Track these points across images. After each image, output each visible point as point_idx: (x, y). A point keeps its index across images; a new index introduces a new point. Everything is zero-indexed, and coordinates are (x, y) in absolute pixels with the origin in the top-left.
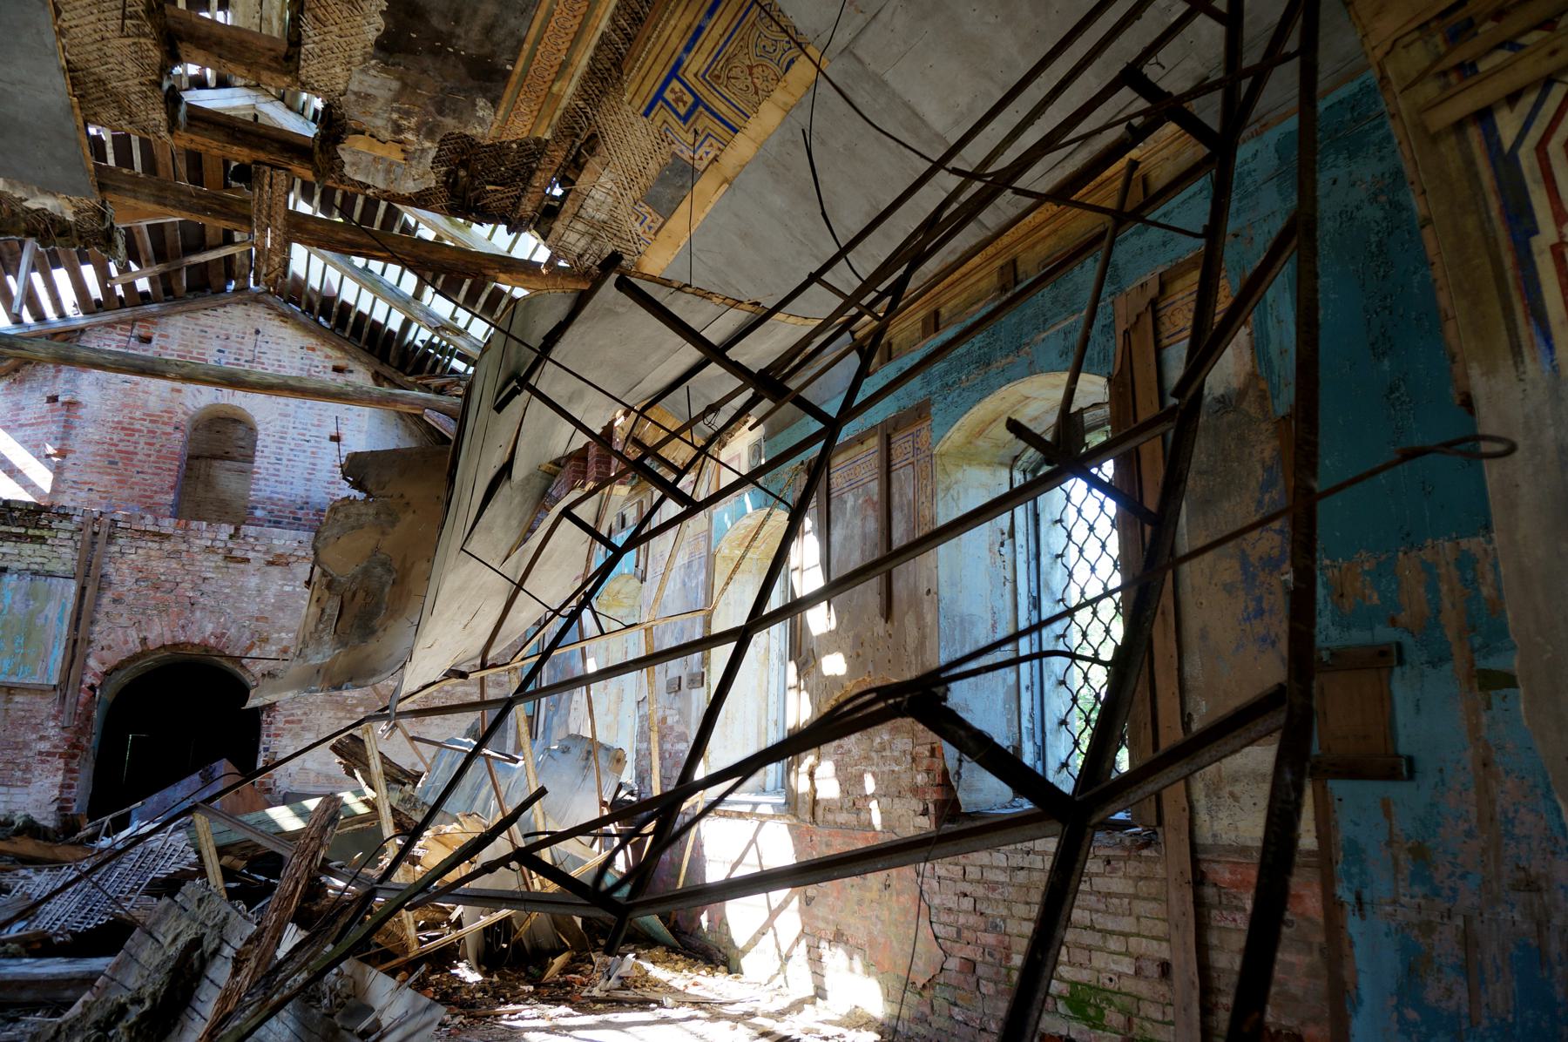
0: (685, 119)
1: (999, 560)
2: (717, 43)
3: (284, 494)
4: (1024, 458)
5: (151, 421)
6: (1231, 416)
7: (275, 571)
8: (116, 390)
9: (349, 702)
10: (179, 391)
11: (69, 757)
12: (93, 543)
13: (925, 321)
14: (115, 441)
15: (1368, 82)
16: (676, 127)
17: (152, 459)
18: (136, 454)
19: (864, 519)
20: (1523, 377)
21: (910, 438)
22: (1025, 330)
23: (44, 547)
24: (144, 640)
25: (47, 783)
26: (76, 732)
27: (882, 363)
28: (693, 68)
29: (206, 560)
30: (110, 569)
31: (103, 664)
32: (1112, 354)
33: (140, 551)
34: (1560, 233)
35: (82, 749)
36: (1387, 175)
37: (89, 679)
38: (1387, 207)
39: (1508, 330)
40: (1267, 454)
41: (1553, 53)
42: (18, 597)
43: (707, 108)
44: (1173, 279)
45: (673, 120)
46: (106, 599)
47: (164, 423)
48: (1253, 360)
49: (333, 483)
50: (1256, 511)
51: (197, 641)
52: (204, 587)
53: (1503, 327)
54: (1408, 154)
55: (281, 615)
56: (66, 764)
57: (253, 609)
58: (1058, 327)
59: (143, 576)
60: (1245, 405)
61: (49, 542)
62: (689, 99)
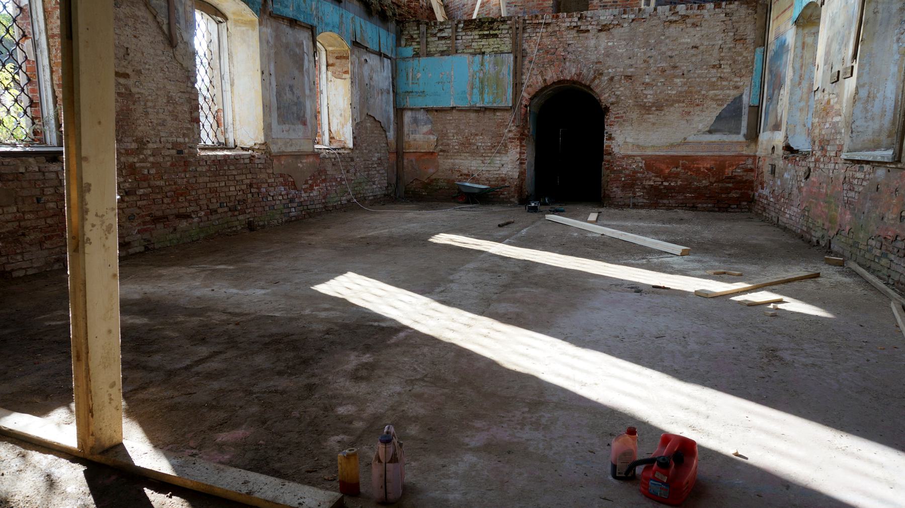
7: (603, 34)
9: (647, 105)
11: (521, 139)
12: (517, 34)
23: (498, 39)
24: (545, 80)
25: (514, 152)
26: (522, 128)
29: (568, 34)
30: (525, 46)
31: (529, 94)
33: (538, 34)
35: (527, 136)
37: (524, 103)
42: (491, 66)
46: (526, 62)
51: (568, 78)
52: (570, 49)
55: (608, 59)
56: (521, 143)
57: (593, 58)
59: (541, 47)
61: (499, 36)
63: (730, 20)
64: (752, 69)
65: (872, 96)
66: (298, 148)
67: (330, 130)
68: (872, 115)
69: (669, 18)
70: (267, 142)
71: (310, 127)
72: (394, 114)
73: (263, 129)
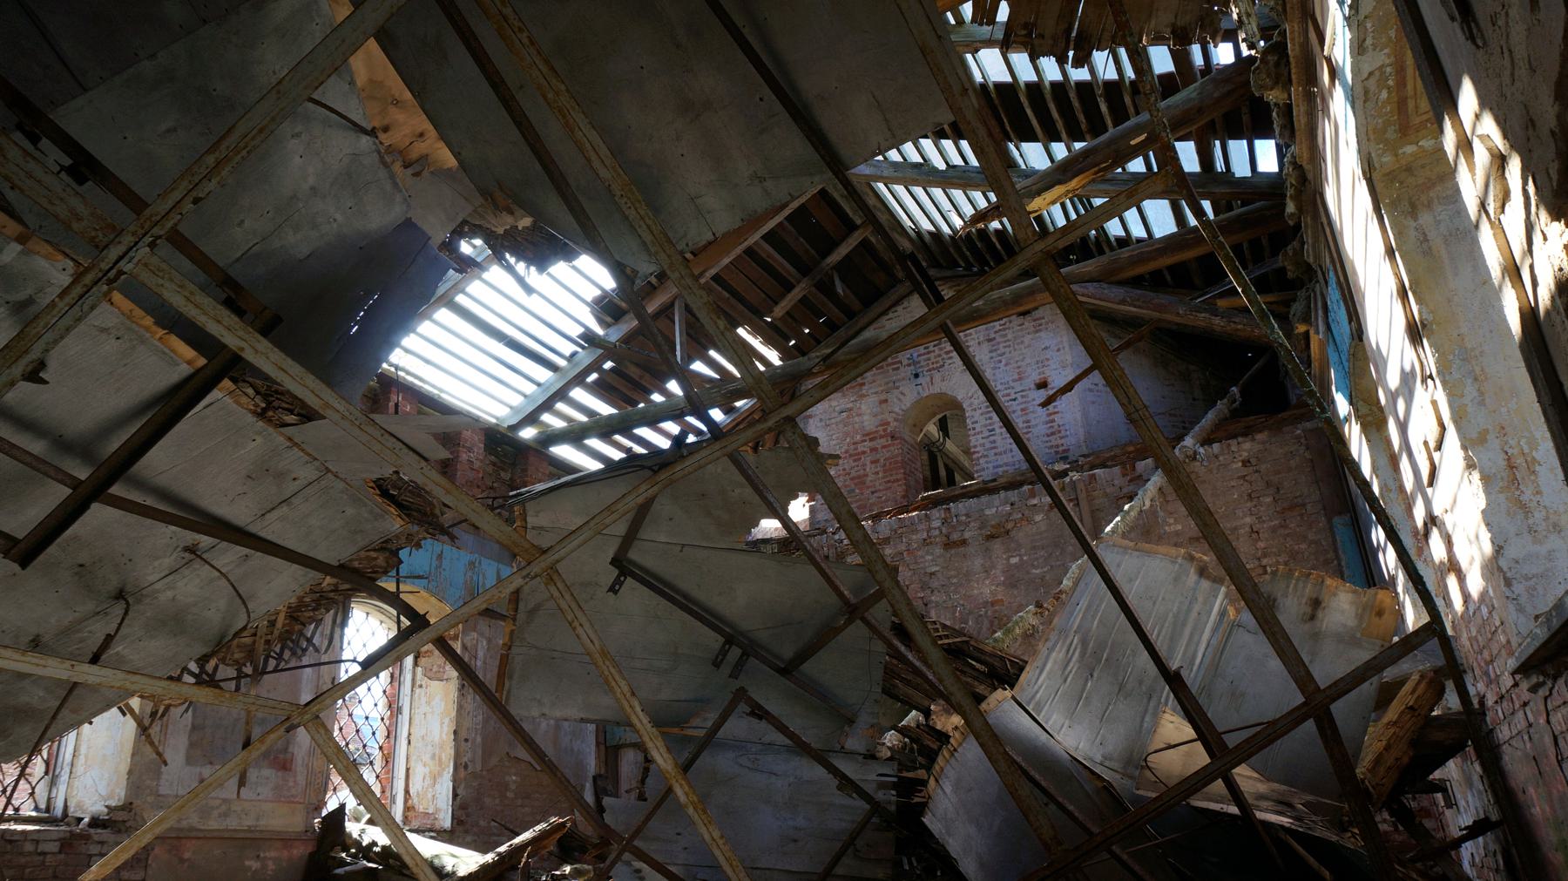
3: (1006, 464)
5: (871, 440)
7: (997, 546)
8: (837, 424)
10: (886, 401)
14: (848, 471)
17: (881, 475)
18: (867, 475)
29: (928, 553)
47: (881, 437)
49: (1053, 434)
52: (935, 584)
63: (1257, 471)
64: (1339, 565)
65: (1520, 461)
66: (248, 822)
67: (407, 792)
68: (1547, 519)
69: (1125, 490)
70: (137, 802)
71: (301, 779)
72: (598, 757)
73: (130, 773)
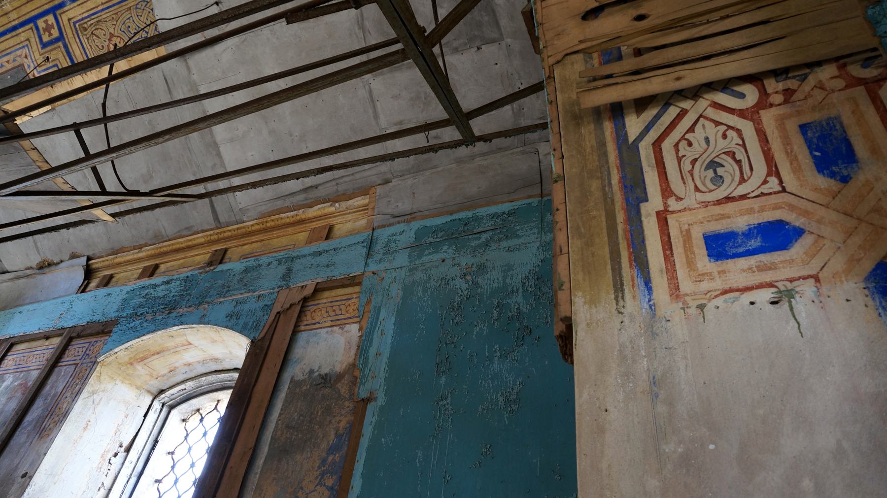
0: (44, 45)
1: (106, 465)
2: (97, 7)
4: (168, 393)
6: (327, 391)
13: (145, 269)
15: (477, 214)
16: (35, 48)
19: (10, 399)
20: (622, 310)
21: (87, 345)
22: (211, 293)
27: (98, 287)
28: (70, 14)
32: (262, 324)
34: (665, 203)
36: (475, 266)
38: (470, 283)
39: (613, 269)
40: (342, 424)
41: (678, 79)
43: (65, 46)
44: (324, 289)
45: (34, 41)
48: (356, 355)
50: (319, 467)
53: (609, 267)
54: (556, 130)
58: (234, 297)
60: (339, 385)
62: (55, 33)
